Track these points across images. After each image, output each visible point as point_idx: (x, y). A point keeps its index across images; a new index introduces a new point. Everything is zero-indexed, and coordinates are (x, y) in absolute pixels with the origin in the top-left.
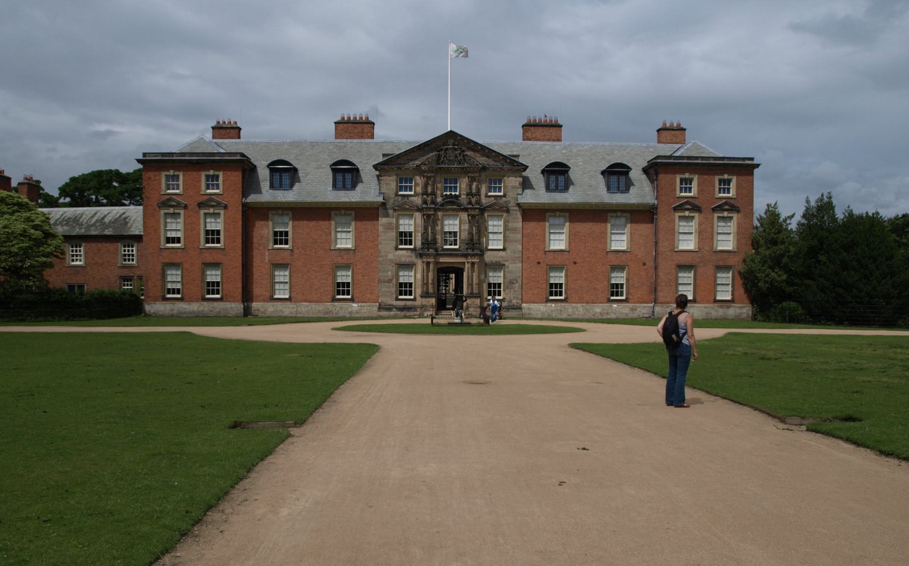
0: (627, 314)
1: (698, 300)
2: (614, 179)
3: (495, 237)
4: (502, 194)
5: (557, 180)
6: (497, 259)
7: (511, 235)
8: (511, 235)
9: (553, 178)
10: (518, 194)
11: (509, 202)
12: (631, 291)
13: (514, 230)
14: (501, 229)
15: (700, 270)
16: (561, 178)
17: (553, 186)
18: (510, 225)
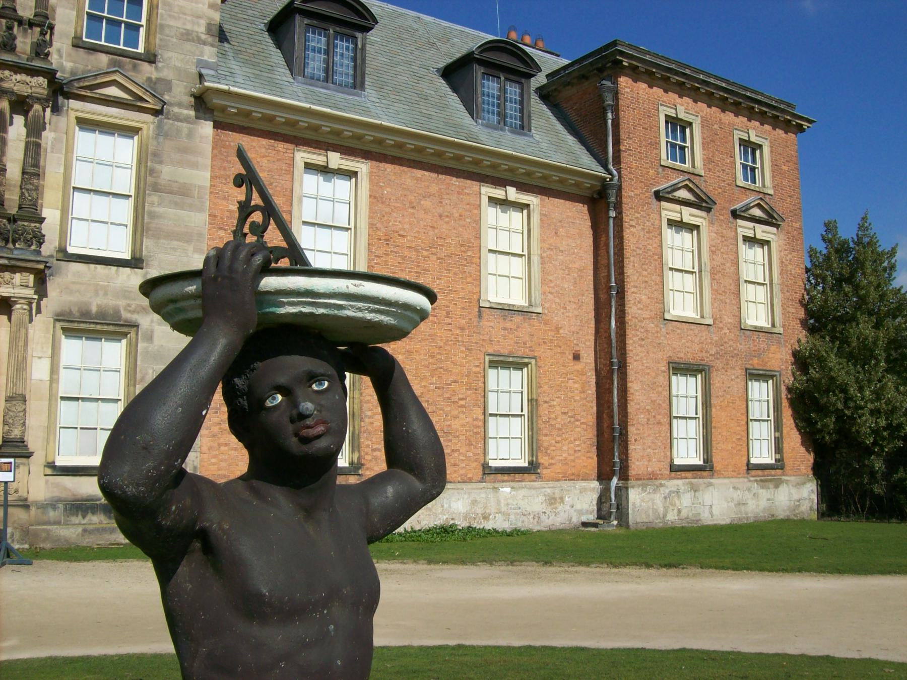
0: (537, 517)
1: (717, 466)
2: (489, 87)
3: (101, 207)
4: (141, 49)
5: (329, 52)
6: (110, 302)
7: (166, 212)
8: (166, 212)
9: (318, 41)
10: (201, 64)
11: (168, 85)
12: (546, 441)
13: (181, 193)
14: (126, 182)
15: (717, 379)
16: (342, 47)
17: (316, 64)
18: (166, 172)
